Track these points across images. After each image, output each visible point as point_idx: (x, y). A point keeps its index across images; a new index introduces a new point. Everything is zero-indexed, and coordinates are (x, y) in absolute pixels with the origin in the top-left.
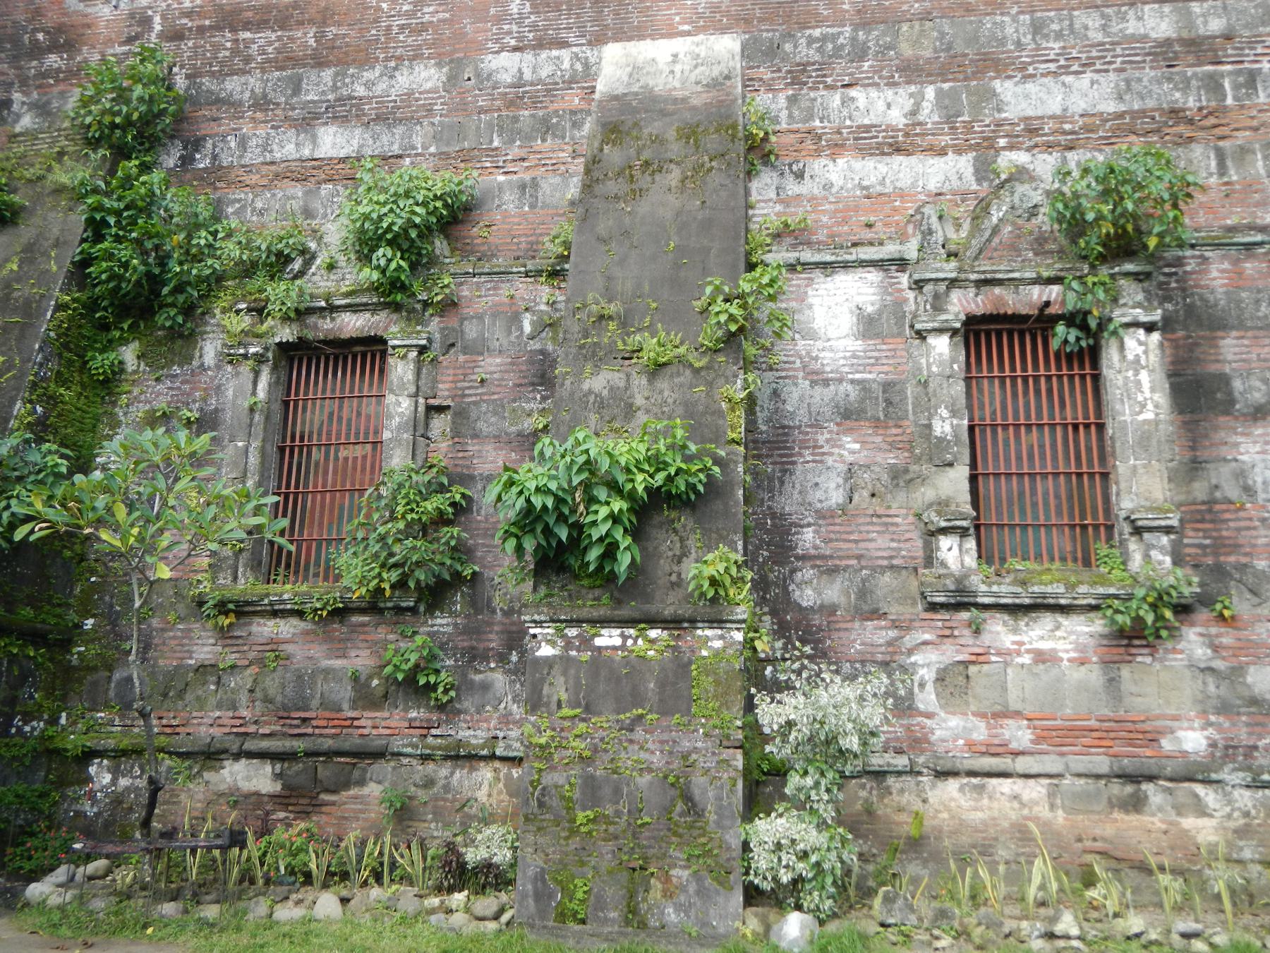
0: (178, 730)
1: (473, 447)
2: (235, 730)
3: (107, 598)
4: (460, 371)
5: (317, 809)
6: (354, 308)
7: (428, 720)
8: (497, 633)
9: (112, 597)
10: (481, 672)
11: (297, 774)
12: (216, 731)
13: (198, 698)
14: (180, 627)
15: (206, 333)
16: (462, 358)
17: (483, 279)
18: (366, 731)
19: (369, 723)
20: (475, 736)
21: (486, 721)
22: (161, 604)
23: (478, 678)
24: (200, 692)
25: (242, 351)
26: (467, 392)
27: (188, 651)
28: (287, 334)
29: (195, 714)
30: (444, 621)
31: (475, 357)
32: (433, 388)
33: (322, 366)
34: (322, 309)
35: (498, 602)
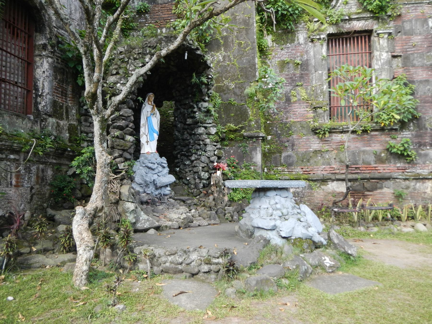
0: (309, 172)
1: (413, 70)
2: (331, 172)
3: (275, 129)
4: (404, 42)
5: (366, 197)
6: (358, 19)
7: (405, 167)
8: (429, 137)
9: (276, 128)
10: (423, 150)
11: (357, 186)
12: (325, 173)
13: (315, 162)
14: (304, 138)
15: (298, 31)
16: (404, 37)
17: (410, 6)
18: (381, 171)
19: (382, 168)
20: (424, 172)
21: (427, 166)
22: (296, 130)
23: (423, 152)
24: (316, 160)
25: (318, 37)
26: (408, 50)
27: (309, 146)
28: (332, 30)
29: (315, 167)
30: (407, 133)
31: (410, 36)
32: (393, 49)
33: (341, 42)
34: (346, 20)
35: (428, 126)
